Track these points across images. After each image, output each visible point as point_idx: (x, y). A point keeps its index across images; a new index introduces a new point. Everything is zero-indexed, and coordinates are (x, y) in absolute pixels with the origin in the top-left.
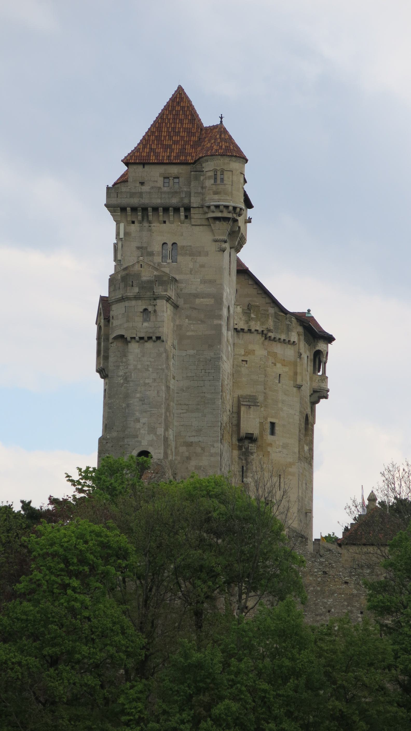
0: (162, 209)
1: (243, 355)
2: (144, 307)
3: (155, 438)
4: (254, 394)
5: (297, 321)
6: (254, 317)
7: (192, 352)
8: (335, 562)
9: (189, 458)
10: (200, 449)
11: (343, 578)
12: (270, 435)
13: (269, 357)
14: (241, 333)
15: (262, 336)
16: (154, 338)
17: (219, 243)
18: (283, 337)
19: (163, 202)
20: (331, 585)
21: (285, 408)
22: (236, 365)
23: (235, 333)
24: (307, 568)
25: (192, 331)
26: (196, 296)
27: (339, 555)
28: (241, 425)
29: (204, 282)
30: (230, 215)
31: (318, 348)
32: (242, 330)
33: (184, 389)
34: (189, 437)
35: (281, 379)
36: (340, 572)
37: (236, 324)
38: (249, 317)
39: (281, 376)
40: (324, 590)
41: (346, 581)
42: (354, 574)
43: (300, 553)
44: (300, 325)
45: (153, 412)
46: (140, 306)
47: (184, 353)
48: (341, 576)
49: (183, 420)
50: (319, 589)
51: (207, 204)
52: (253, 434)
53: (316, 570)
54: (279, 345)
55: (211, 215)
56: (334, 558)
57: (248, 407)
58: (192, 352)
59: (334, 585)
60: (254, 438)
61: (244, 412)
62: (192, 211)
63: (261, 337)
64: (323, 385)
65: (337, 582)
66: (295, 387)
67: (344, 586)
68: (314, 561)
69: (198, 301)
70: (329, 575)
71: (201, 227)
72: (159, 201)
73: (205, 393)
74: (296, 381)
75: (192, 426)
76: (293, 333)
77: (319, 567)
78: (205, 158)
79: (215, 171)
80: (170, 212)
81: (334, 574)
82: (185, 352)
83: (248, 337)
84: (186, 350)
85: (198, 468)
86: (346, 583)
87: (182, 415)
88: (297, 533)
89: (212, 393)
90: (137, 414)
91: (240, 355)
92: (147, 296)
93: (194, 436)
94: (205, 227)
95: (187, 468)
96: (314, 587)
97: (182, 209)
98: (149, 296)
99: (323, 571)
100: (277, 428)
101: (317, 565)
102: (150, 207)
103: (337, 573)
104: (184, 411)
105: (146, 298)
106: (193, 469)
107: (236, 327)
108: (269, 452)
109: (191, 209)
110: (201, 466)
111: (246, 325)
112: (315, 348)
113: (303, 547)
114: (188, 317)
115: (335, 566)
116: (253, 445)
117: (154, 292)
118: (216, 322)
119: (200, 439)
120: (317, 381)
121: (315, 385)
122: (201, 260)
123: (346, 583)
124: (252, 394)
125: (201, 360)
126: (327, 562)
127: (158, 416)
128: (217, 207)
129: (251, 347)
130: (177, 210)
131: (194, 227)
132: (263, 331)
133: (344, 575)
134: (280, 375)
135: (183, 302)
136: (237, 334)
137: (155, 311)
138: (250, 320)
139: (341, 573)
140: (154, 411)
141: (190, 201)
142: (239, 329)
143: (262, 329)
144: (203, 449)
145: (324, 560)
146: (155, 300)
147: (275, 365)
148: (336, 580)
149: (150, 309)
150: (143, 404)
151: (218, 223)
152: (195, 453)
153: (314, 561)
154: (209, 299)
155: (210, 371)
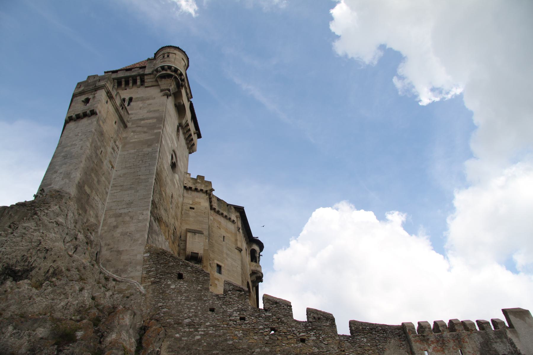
0: (124, 79)
1: (191, 204)
2: (86, 97)
3: (67, 181)
4: (200, 230)
5: (236, 210)
6: (200, 181)
7: (133, 151)
8: (285, 316)
9: (116, 227)
10: (129, 217)
11: (298, 334)
12: (217, 272)
13: (215, 222)
14: (190, 192)
15: (207, 195)
16: (88, 112)
17: (164, 92)
18: (225, 213)
19: (125, 75)
20: (283, 344)
21: (228, 259)
22: (185, 209)
23: (185, 191)
24: (249, 325)
25: (136, 139)
26: (143, 119)
27: (289, 307)
28: (187, 246)
29: (150, 112)
30: (173, 74)
31: (252, 248)
32: (190, 188)
33: (122, 175)
34: (120, 209)
35: (225, 239)
36: (292, 327)
37: (186, 184)
38: (196, 181)
39: (225, 238)
40: (275, 351)
41: (302, 337)
42: (310, 328)
43: (239, 308)
44: (238, 212)
45: (73, 162)
46: (83, 97)
47: (126, 153)
48: (295, 332)
49: (115, 198)
50: (267, 349)
51: (156, 68)
52: (198, 254)
53: (261, 327)
54: (222, 218)
55: (159, 74)
56: (283, 311)
57: (193, 234)
58: (133, 151)
59: (287, 344)
60: (199, 257)
61: (190, 237)
62: (146, 77)
63: (205, 195)
64: (259, 269)
65: (290, 340)
66: (236, 249)
67: (300, 344)
68: (257, 316)
69: (143, 122)
70: (279, 332)
71: (152, 88)
72: (123, 76)
73: (140, 176)
74: (237, 244)
75: (124, 201)
76: (232, 215)
77: (265, 323)
78: (157, 53)
79: (164, 54)
80: (130, 80)
81: (285, 331)
82: (127, 152)
83: (195, 194)
84: (128, 151)
85: (124, 234)
86: (303, 340)
87: (115, 194)
88: (234, 286)
89: (147, 175)
90: (57, 167)
91: (189, 204)
92: (89, 89)
93: (125, 208)
94: (154, 87)
95: (113, 235)
96: (261, 348)
97: (138, 78)
98: (91, 89)
99: (271, 327)
100: (223, 270)
101: (263, 321)
102: (116, 79)
103: (289, 329)
104: (118, 191)
105: (89, 92)
106: (119, 235)
107: (185, 185)
108: (216, 284)
109: (145, 76)
110: (127, 232)
111: (194, 185)
112: (251, 247)
113: (242, 301)
114: (133, 132)
115: (285, 321)
116: (199, 265)
117: (96, 85)
118: (156, 131)
119: (130, 210)
120: (254, 266)
121: (253, 268)
122: (148, 102)
123: (303, 340)
124: (198, 229)
125: (140, 155)
126: (274, 317)
127: (76, 164)
128: (163, 68)
129: (197, 200)
130: (135, 82)
131: (146, 88)
132: (206, 191)
133: (299, 330)
134: (224, 237)
135: (131, 124)
136: (187, 191)
137: (94, 97)
138: (196, 183)
139: (294, 329)
140: (73, 161)
141: (144, 72)
142: (188, 186)
143: (206, 189)
144: (132, 218)
145: (270, 315)
146: (96, 91)
147: (220, 228)
148: (289, 337)
149: (91, 97)
150: (65, 159)
151: (164, 80)
152: (122, 222)
153: (257, 316)
154: (153, 120)
155: (147, 161)
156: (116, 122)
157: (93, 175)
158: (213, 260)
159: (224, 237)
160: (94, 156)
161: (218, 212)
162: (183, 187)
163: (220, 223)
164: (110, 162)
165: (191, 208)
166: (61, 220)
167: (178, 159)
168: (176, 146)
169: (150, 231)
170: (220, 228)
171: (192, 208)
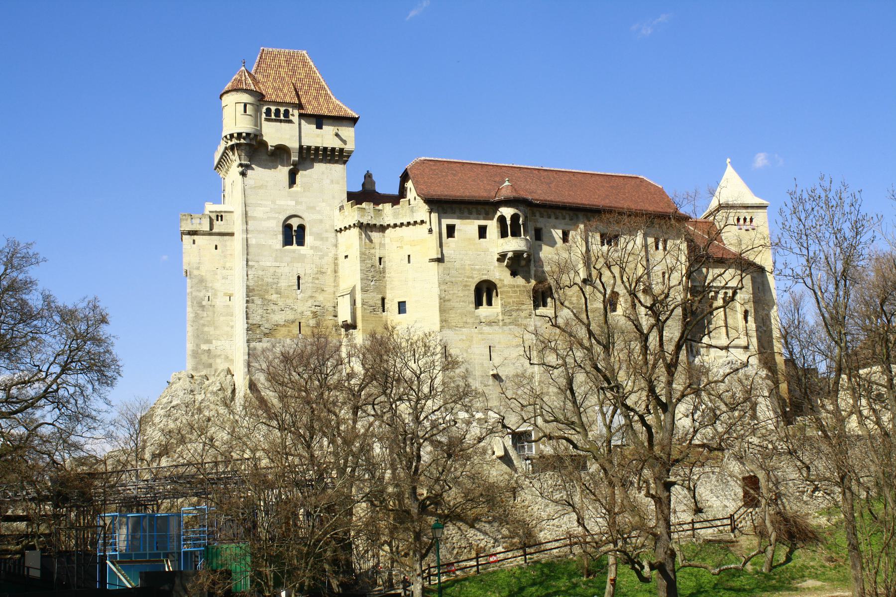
32: (341, 230)
134: (409, 256)
142: (338, 229)
156: (216, 246)
157: (206, 329)
158: (392, 300)
159: (409, 256)
160: (200, 312)
161: (395, 226)
162: (334, 234)
163: (401, 239)
164: (225, 294)
165: (346, 257)
166: (174, 403)
167: (303, 216)
168: (293, 203)
169: (251, 360)
170: (401, 247)
171: (346, 257)
